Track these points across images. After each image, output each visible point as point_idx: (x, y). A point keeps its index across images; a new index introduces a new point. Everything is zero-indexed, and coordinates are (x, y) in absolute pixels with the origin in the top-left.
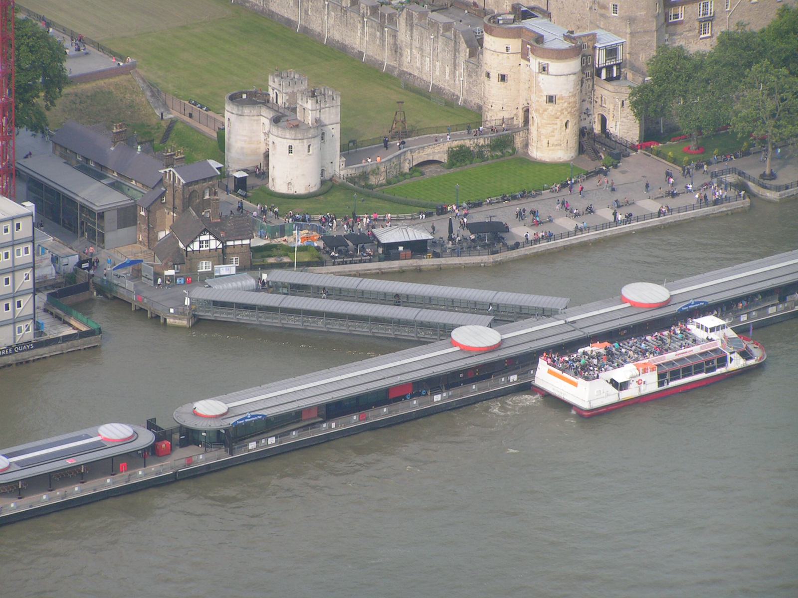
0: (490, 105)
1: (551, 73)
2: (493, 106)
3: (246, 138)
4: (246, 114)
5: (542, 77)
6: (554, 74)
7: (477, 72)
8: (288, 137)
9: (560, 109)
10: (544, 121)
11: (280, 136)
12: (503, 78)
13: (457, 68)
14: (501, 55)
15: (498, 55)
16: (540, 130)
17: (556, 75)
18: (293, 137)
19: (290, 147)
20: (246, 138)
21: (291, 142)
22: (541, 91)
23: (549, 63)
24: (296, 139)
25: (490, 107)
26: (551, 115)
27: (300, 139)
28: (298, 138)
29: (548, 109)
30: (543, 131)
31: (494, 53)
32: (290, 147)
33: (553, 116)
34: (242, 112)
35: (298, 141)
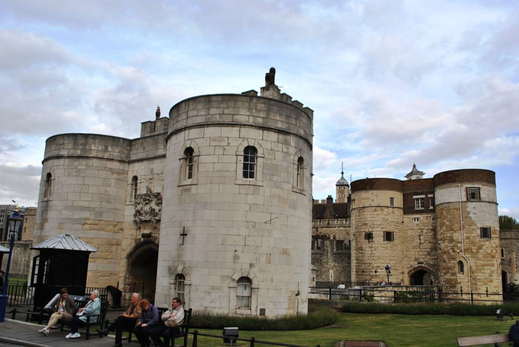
0: (374, 270)
1: (483, 200)
2: (379, 270)
3: (86, 214)
4: (94, 154)
5: (471, 206)
6: (487, 200)
7: (321, 260)
8: (242, 119)
9: (494, 246)
10: (481, 262)
11: (217, 119)
12: (389, 236)
14: (386, 210)
15: (382, 210)
16: (475, 274)
17: (488, 202)
18: (260, 121)
19: (250, 152)
20: (86, 214)
21: (254, 137)
22: (472, 223)
23: (480, 186)
24: (269, 129)
25: (374, 273)
26: (487, 254)
27: (279, 131)
28: (271, 124)
29: (483, 245)
30: (480, 276)
31: (378, 209)
32: (250, 152)
33: (490, 254)
34: (83, 150)
35: (273, 136)
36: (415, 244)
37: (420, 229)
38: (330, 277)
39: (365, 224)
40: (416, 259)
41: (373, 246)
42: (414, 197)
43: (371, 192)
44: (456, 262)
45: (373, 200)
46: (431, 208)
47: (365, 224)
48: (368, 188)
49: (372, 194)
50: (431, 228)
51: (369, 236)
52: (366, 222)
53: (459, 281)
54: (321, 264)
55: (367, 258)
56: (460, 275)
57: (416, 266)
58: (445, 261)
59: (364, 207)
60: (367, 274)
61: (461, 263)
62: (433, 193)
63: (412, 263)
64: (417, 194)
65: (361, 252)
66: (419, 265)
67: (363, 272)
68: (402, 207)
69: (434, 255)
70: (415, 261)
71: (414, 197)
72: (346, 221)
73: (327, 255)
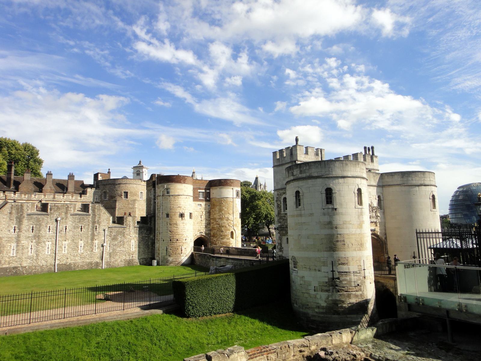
0: (184, 239)
2: (187, 239)
13: (96, 237)
25: (185, 241)
36: (199, 221)
37: (201, 211)
38: (132, 246)
39: (179, 207)
40: (199, 230)
41: (185, 222)
42: (199, 191)
43: (184, 185)
44: (230, 232)
45: (185, 191)
46: (208, 199)
47: (179, 207)
48: (182, 182)
49: (185, 186)
50: (208, 211)
51: (182, 215)
52: (180, 206)
53: (231, 242)
54: (124, 236)
55: (180, 230)
56: (231, 239)
57: (199, 235)
58: (222, 231)
59: (179, 195)
60: (180, 241)
61: (232, 233)
62: (209, 189)
63: (196, 233)
64: (200, 189)
65: (176, 226)
66: (200, 234)
67: (177, 240)
68: (192, 195)
69: (209, 228)
70: (198, 231)
71: (199, 191)
72: (72, 197)
73: (129, 228)
